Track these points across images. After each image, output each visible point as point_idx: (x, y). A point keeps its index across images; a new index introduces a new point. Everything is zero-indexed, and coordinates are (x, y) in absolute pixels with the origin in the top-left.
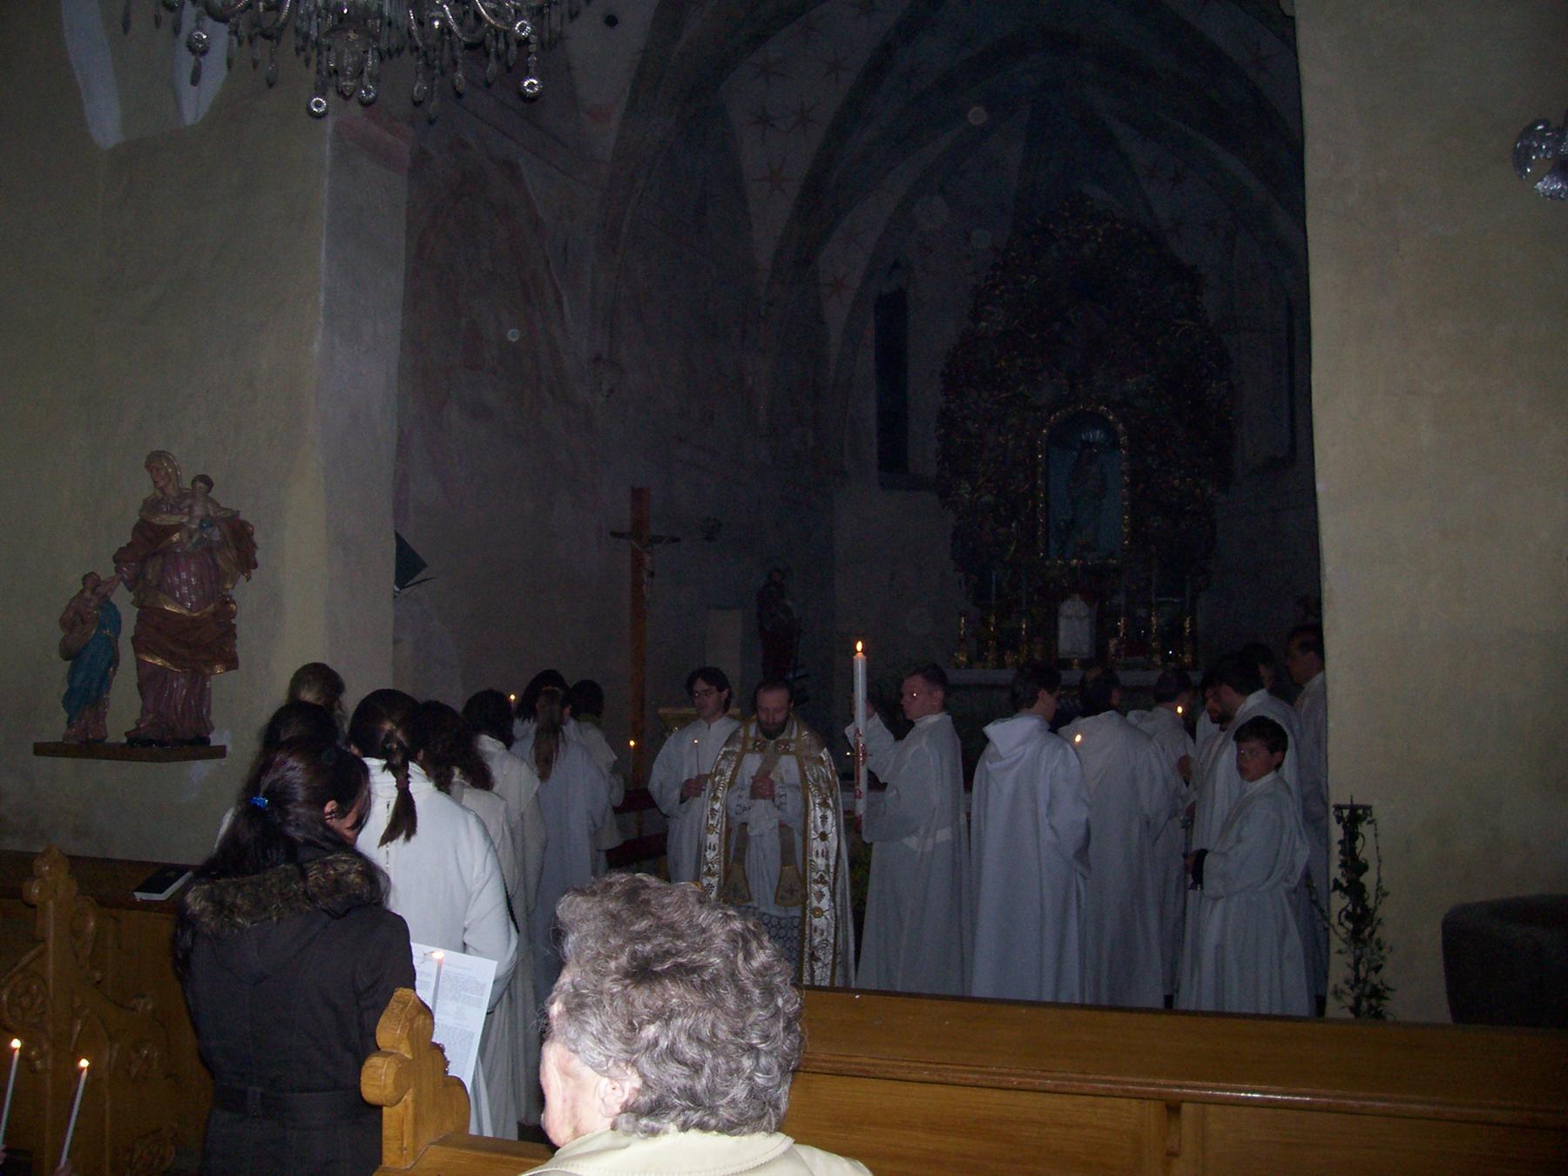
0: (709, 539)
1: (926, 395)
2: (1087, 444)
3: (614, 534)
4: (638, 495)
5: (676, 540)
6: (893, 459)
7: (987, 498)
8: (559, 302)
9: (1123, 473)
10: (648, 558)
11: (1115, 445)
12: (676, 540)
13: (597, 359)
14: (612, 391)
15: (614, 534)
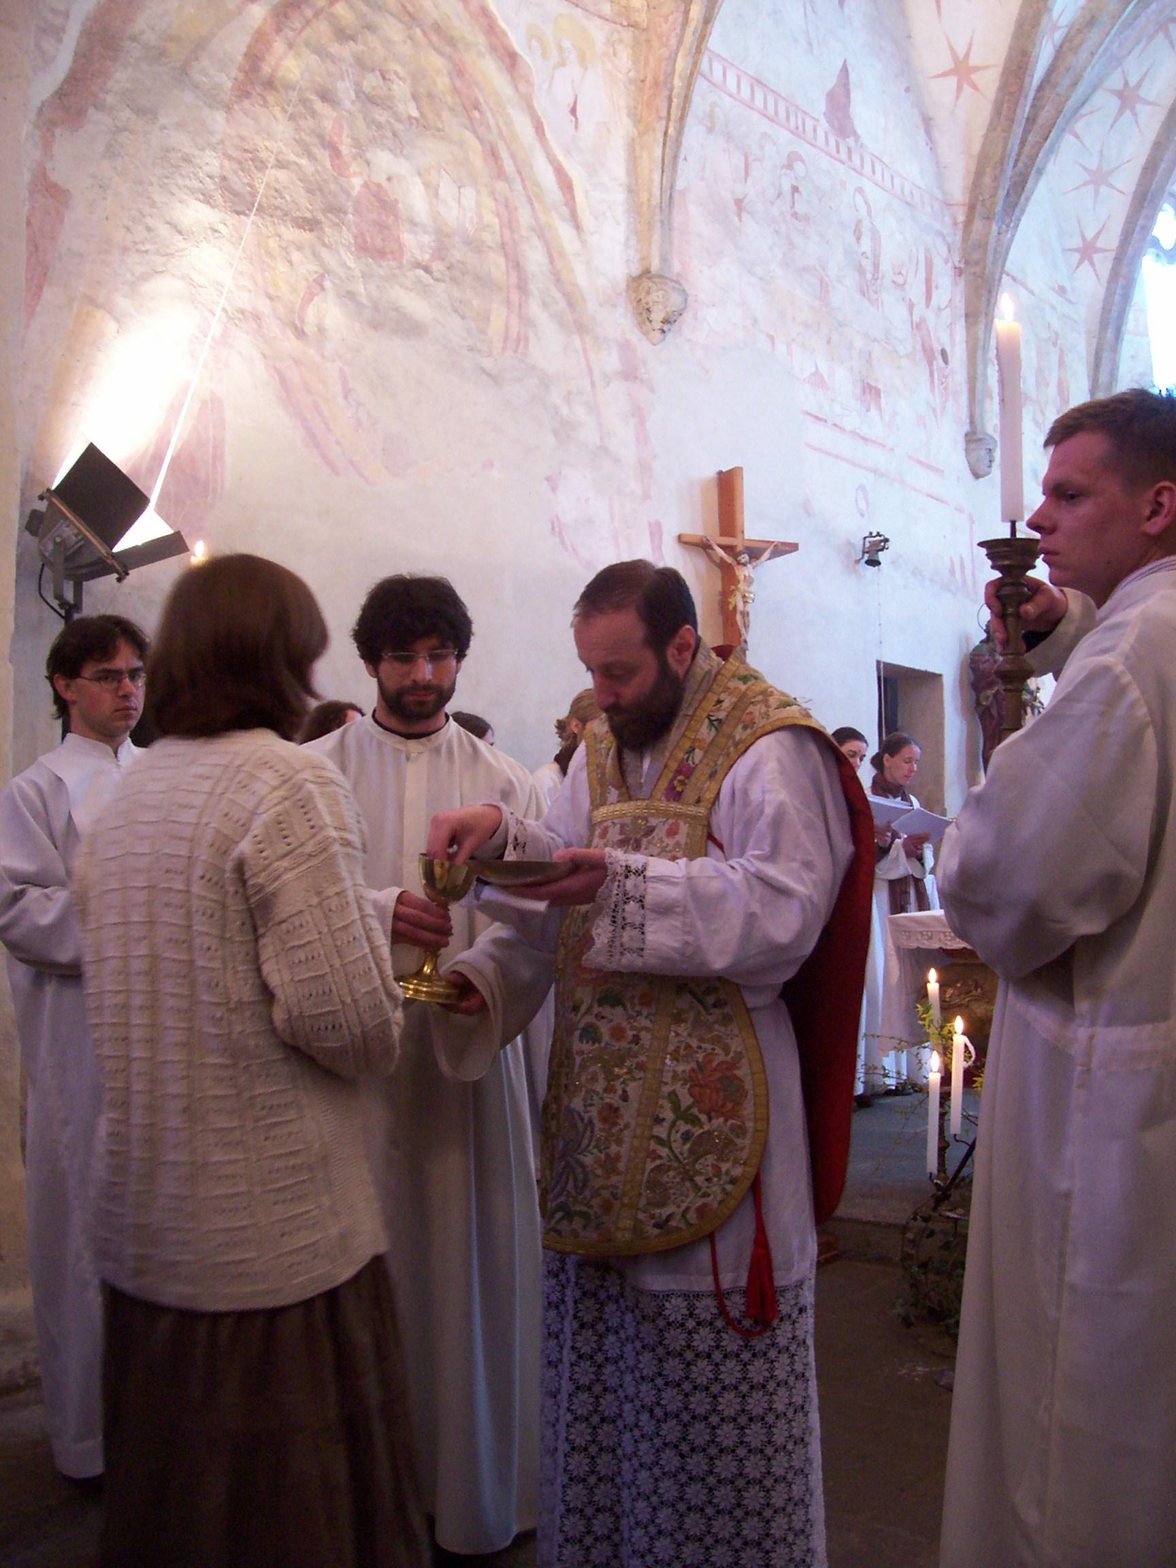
0: (873, 562)
5: (793, 547)
10: (742, 573)
13: (646, 273)
14: (666, 321)
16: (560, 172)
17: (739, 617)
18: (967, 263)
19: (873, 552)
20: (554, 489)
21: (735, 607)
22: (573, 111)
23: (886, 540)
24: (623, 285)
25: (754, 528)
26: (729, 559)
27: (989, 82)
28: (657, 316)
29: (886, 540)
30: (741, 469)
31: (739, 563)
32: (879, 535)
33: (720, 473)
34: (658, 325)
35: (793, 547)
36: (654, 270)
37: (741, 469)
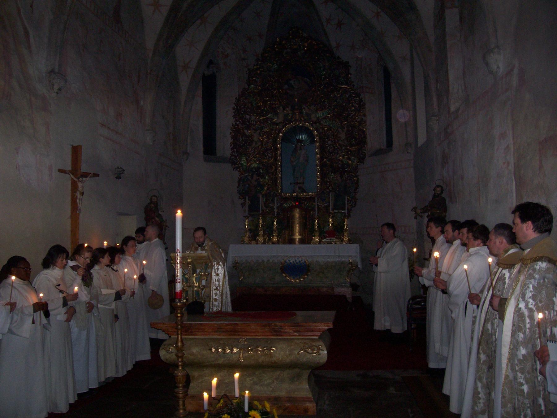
0: (118, 178)
1: (225, 119)
2: (300, 141)
3: (60, 171)
4: (76, 151)
5: (98, 175)
6: (210, 148)
7: (255, 165)
8: (27, 34)
9: (317, 153)
10: (80, 184)
11: (313, 141)
12: (97, 175)
13: (52, 71)
14: (60, 89)
15: (60, 171)
16: (25, 29)
17: (78, 201)
18: (151, 71)
19: (119, 175)
20: (17, 153)
21: (77, 197)
22: (32, 6)
23: (124, 170)
24: (44, 75)
25: (84, 168)
26: (75, 179)
27: (165, 11)
28: (56, 87)
29: (124, 170)
30: (81, 147)
31: (79, 181)
32: (121, 168)
33: (73, 146)
34: (56, 91)
35: (98, 175)
36: (56, 70)
37: (81, 147)
